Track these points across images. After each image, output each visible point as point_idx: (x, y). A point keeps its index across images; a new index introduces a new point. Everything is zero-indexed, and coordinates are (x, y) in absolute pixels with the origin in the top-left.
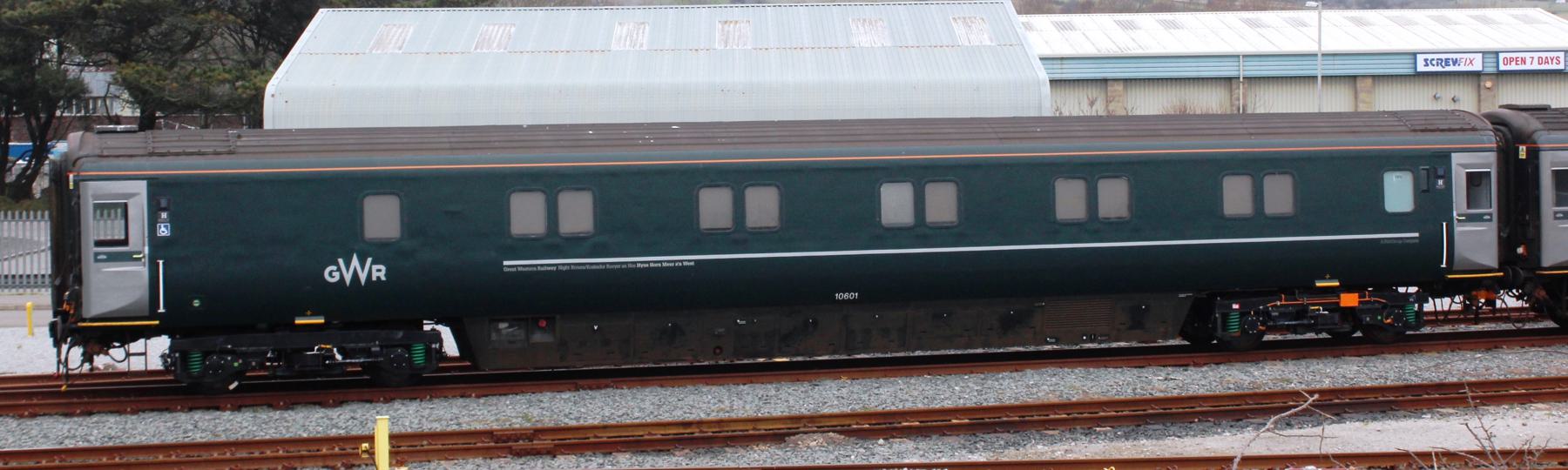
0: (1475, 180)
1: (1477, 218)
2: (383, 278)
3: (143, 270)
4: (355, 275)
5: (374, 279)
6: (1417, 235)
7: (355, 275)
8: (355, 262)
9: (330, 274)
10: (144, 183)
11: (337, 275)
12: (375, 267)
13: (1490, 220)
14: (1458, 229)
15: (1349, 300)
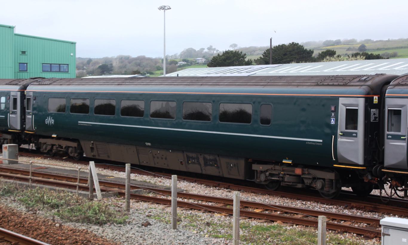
0: (352, 115)
1: (349, 135)
3: (31, 117)
6: (321, 141)
10: (32, 92)
13: (356, 136)
14: (340, 140)
15: (298, 171)
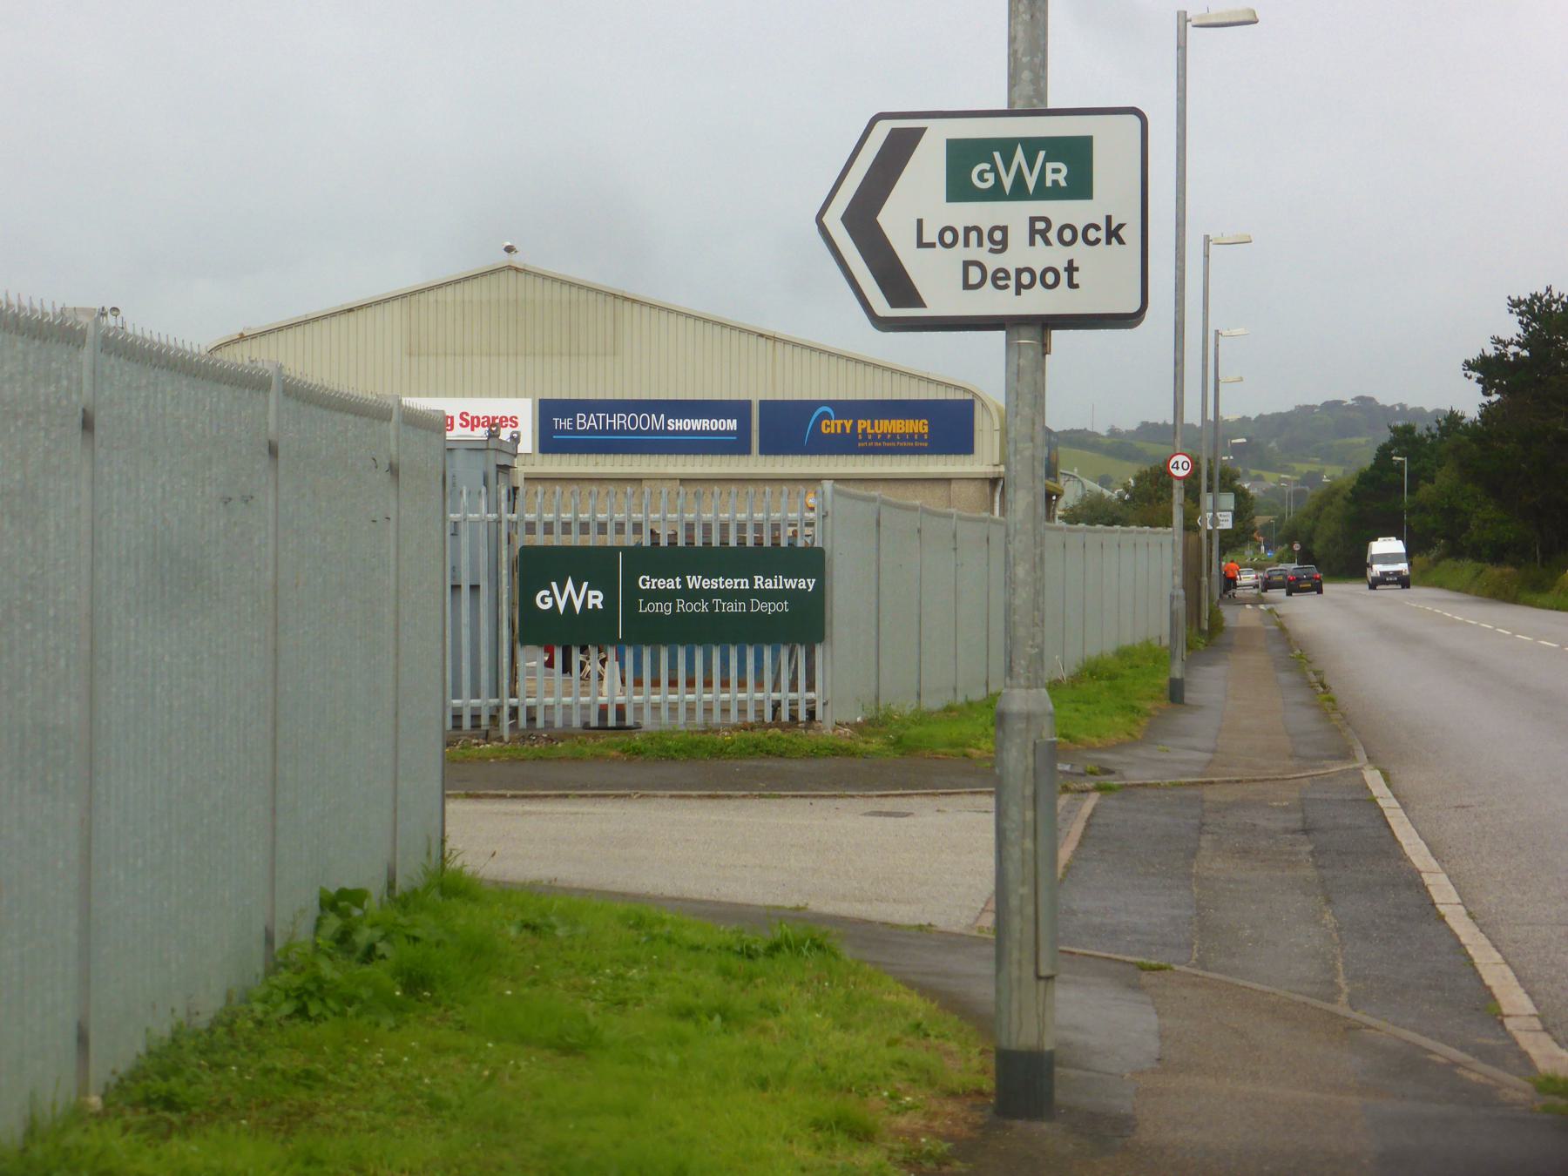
2: (600, 607)
4: (570, 601)
5: (590, 607)
7: (570, 601)
8: (570, 586)
9: (543, 600)
11: (549, 600)
12: (591, 593)
